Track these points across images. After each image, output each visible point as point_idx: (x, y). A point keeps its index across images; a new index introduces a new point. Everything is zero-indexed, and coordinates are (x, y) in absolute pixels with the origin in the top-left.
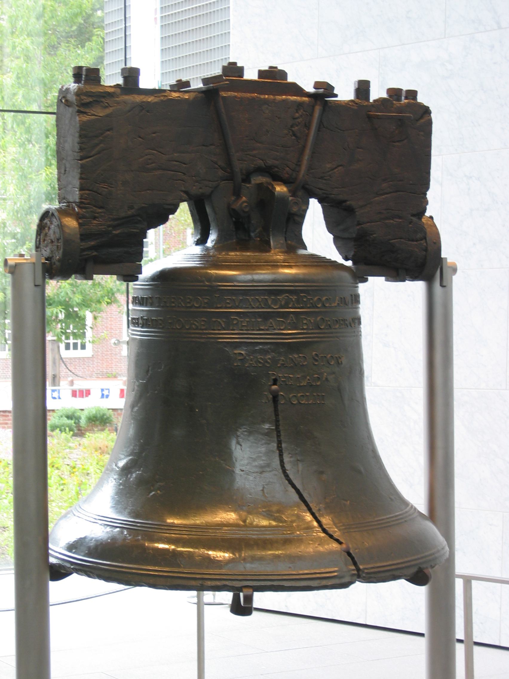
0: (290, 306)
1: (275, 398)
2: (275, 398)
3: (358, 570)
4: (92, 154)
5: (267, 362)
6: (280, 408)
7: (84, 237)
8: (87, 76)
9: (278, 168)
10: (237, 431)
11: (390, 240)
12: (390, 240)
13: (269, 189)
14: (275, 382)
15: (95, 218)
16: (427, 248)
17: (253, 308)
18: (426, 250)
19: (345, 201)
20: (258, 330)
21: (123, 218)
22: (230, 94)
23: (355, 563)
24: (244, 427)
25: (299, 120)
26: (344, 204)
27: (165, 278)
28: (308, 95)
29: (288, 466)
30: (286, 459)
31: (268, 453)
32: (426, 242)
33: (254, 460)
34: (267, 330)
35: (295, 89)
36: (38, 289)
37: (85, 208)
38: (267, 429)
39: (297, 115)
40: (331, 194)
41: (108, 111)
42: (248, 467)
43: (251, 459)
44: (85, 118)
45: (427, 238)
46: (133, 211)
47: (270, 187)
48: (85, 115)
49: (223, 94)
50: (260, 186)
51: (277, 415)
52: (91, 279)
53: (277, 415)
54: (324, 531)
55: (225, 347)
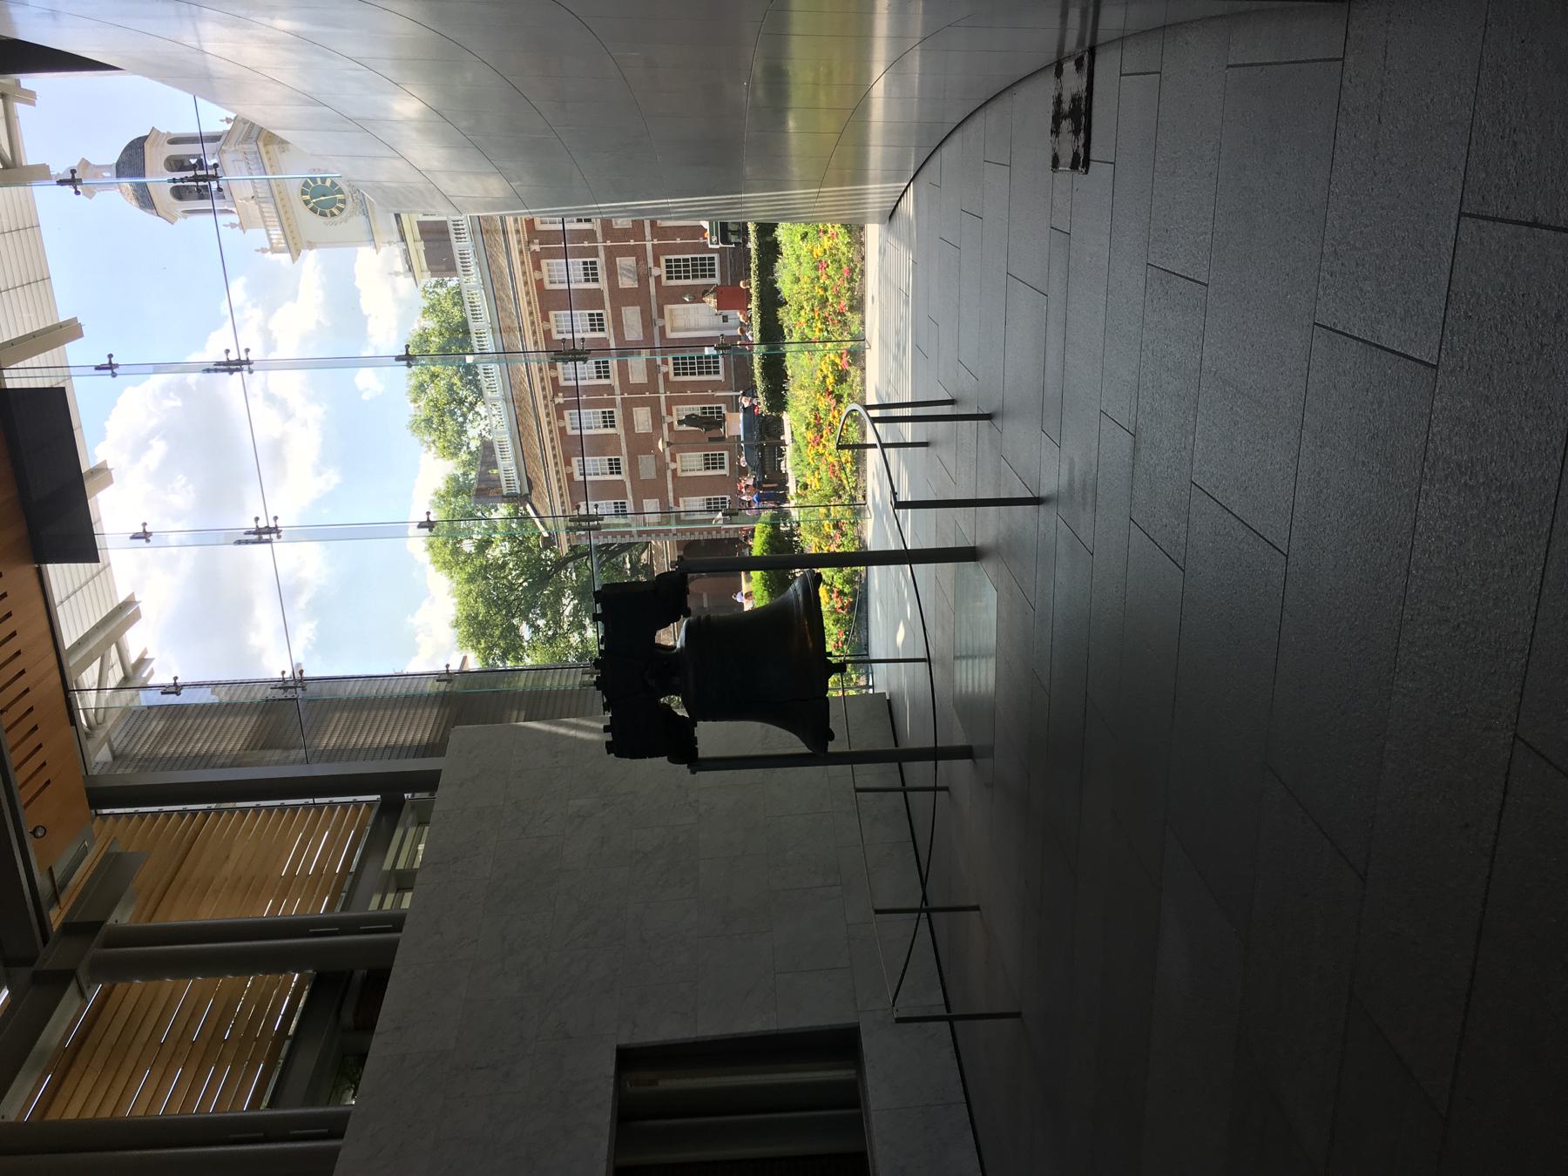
8: (610, 747)
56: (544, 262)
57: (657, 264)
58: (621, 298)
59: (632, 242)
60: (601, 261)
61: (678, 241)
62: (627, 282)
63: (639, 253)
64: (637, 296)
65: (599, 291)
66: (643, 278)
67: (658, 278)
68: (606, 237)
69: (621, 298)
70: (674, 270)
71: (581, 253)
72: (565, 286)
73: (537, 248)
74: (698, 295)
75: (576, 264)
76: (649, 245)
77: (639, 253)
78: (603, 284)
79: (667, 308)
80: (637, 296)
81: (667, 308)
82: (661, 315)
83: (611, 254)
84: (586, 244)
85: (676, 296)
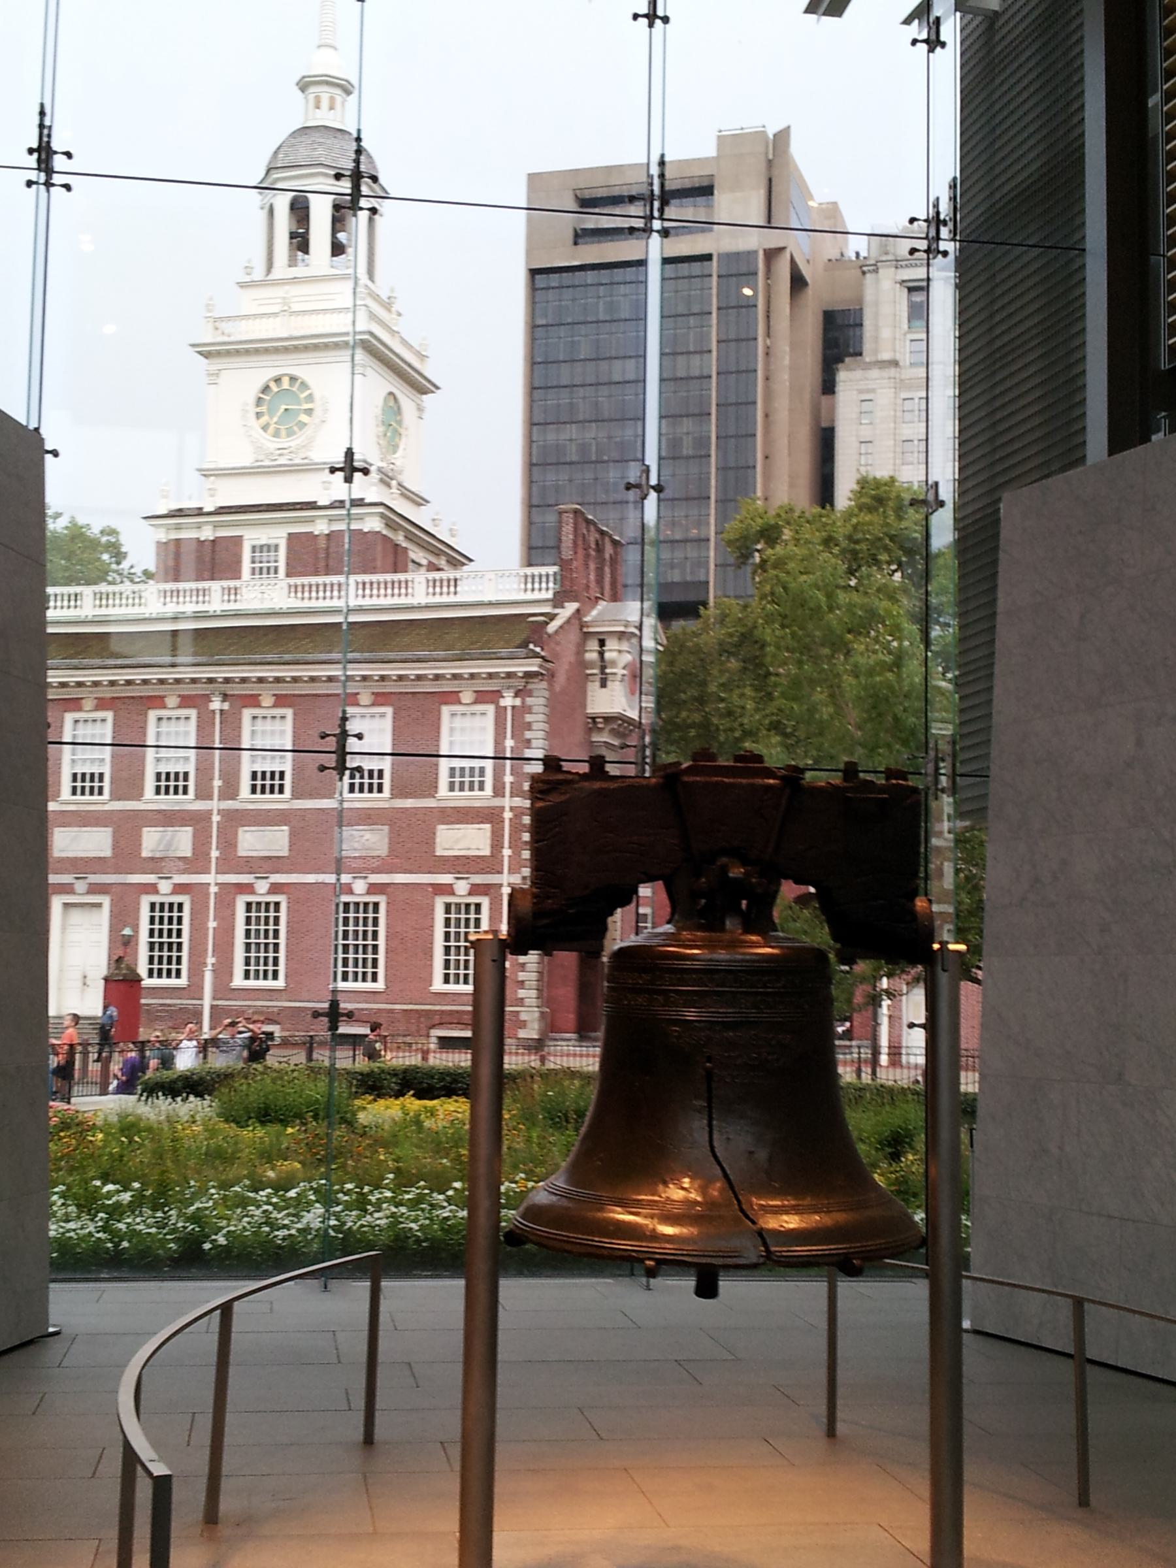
1: (709, 1075)
2: (709, 1075)
3: (767, 1250)
7: (538, 914)
14: (709, 1059)
15: (549, 898)
22: (692, 779)
23: (765, 1244)
27: (623, 954)
29: (716, 1144)
30: (716, 1136)
35: (769, 773)
41: (563, 798)
44: (540, 804)
49: (686, 779)
51: (710, 1090)
52: (551, 955)
53: (710, 1090)
54: (742, 1210)
56: (193, 713)
57: (179, 889)
58: (127, 828)
59: (215, 854)
60: (188, 802)
61: (212, 924)
62: (151, 840)
63: (197, 861)
64: (126, 854)
65: (139, 795)
66: (155, 864)
67: (152, 889)
68: (227, 815)
69: (127, 828)
70: (166, 915)
71: (204, 771)
72: (151, 741)
73: (216, 704)
74: (121, 945)
75: (188, 763)
76: (209, 878)
77: (197, 861)
78: (150, 800)
79: (106, 901)
80: (126, 854)
81: (106, 901)
82: (94, 889)
83: (198, 821)
84: (217, 783)
85: (122, 916)
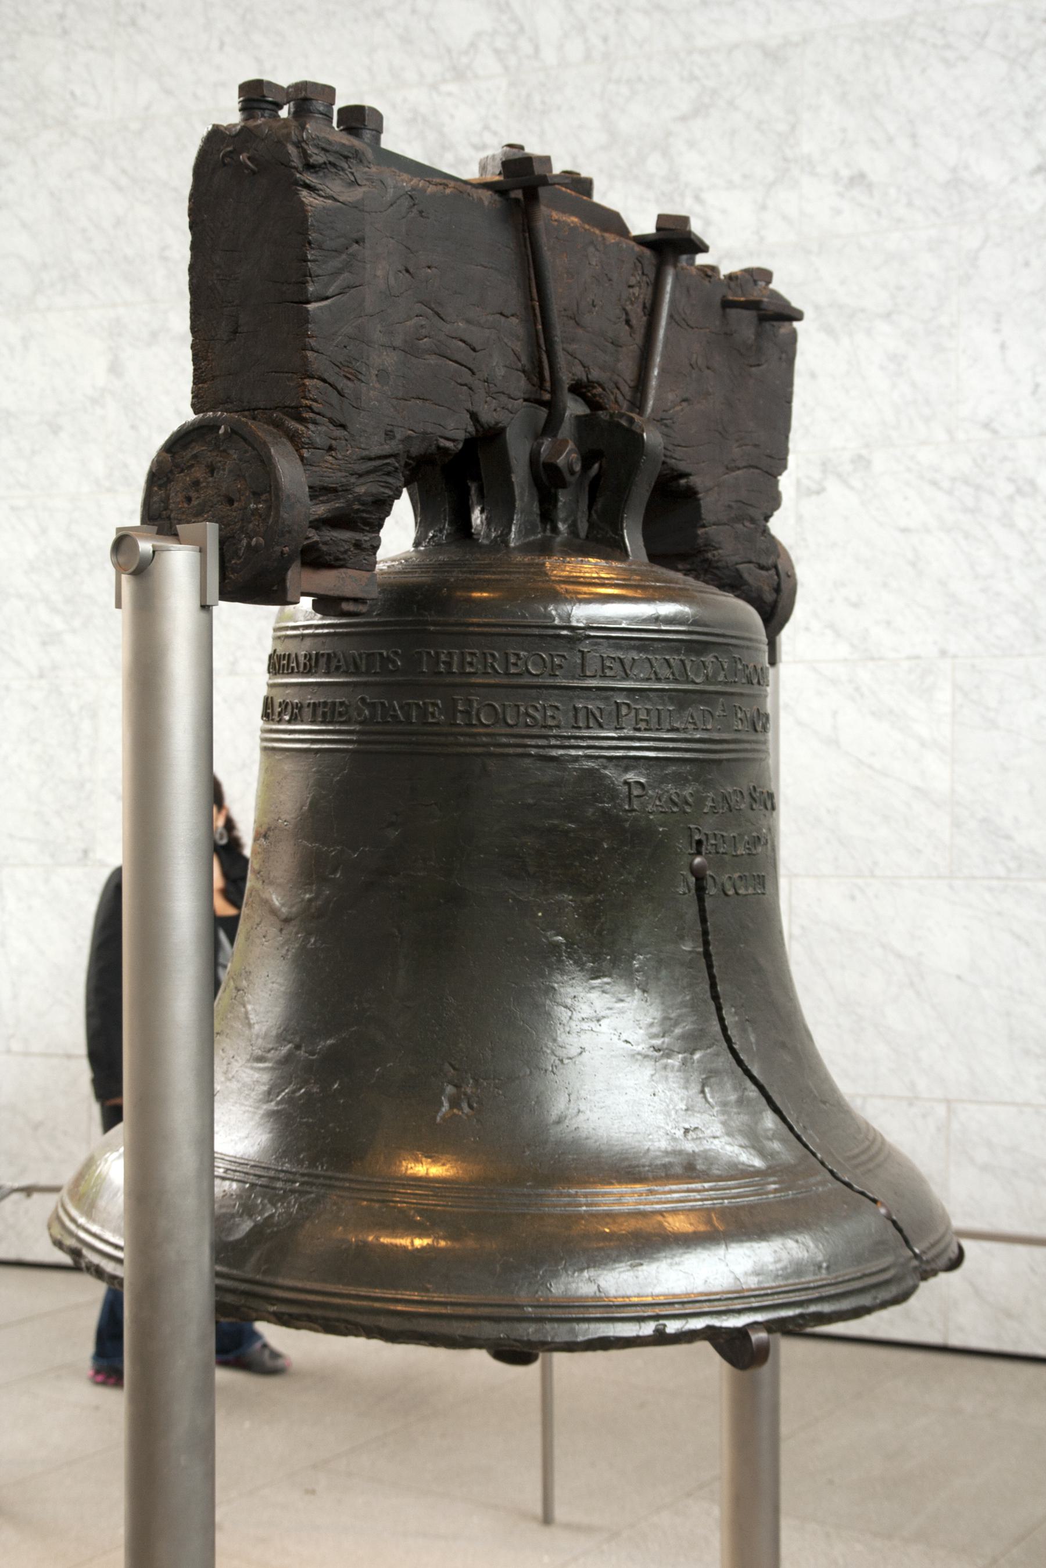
0: (719, 679)
4: (331, 291)
5: (687, 803)
6: (708, 904)
7: (317, 492)
9: (604, 389)
10: (634, 958)
11: (737, 564)
12: (737, 564)
13: (622, 425)
16: (779, 584)
17: (658, 680)
18: (778, 590)
19: (686, 475)
20: (668, 731)
21: (380, 458)
24: (648, 949)
25: (636, 290)
26: (683, 481)
28: (642, 241)
31: (694, 1006)
32: (778, 574)
33: (676, 1024)
34: (685, 730)
36: (203, 615)
37: (315, 423)
38: (690, 952)
39: (633, 281)
40: (671, 457)
42: (667, 1040)
43: (668, 1023)
45: (780, 567)
46: (393, 443)
47: (624, 423)
48: (314, 195)
50: (580, 421)
55: (605, 768)
